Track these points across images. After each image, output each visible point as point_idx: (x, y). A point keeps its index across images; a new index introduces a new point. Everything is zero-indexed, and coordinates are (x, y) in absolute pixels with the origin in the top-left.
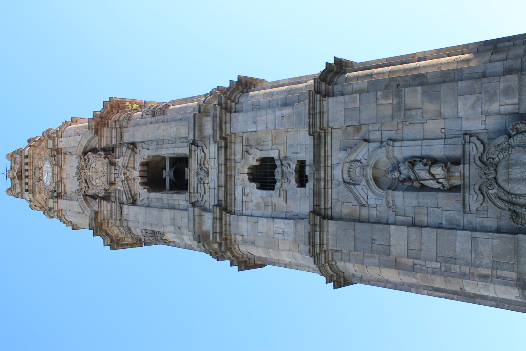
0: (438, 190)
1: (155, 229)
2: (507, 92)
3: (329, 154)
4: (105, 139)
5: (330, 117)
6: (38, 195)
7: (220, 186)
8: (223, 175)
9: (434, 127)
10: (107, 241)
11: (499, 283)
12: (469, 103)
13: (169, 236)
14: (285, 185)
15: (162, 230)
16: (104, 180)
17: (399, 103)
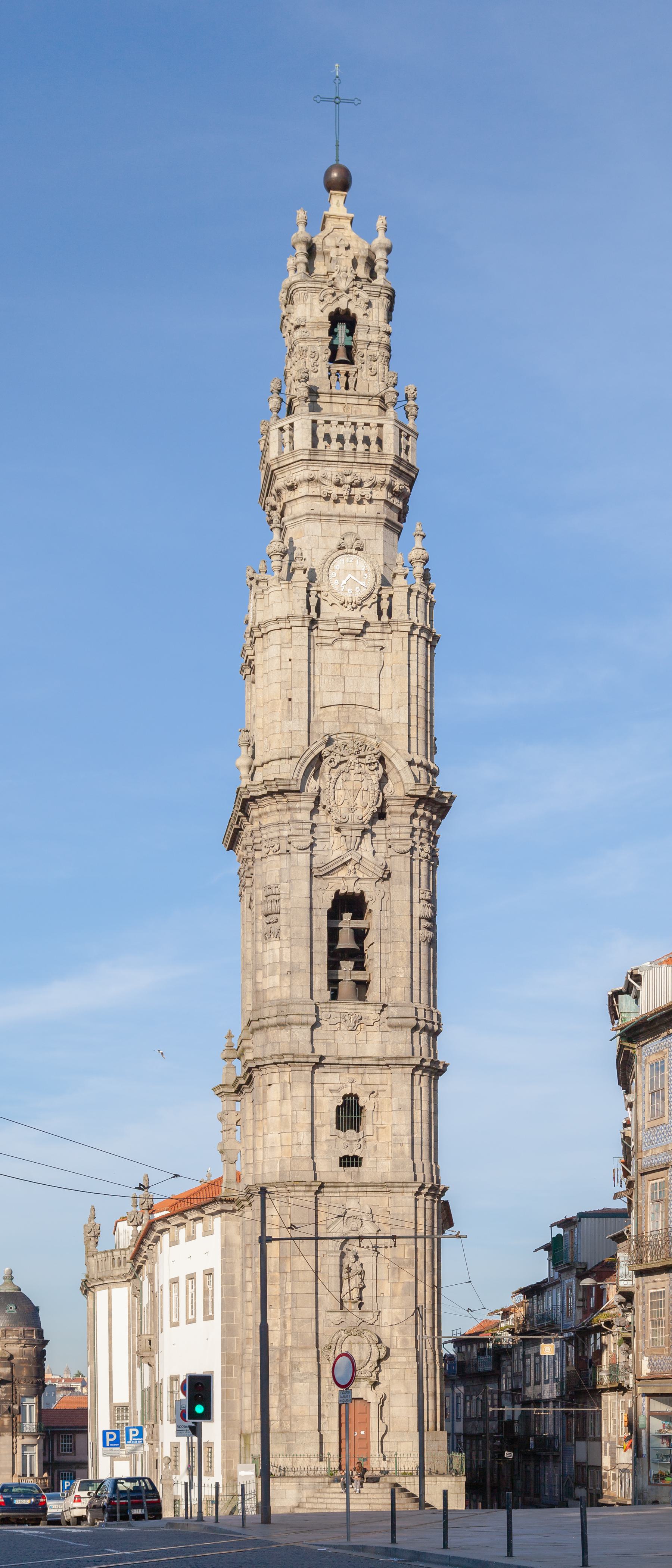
0: (341, 1292)
1: (282, 918)
2: (405, 1341)
3: (368, 1194)
4: (399, 809)
5: (399, 1199)
6: (306, 475)
7: (339, 1058)
8: (350, 1062)
9: (386, 1288)
10: (254, 791)
11: (282, 1335)
12: (399, 1316)
13: (275, 944)
14: (341, 1142)
15: (284, 937)
16: (343, 810)
17: (404, 1263)
